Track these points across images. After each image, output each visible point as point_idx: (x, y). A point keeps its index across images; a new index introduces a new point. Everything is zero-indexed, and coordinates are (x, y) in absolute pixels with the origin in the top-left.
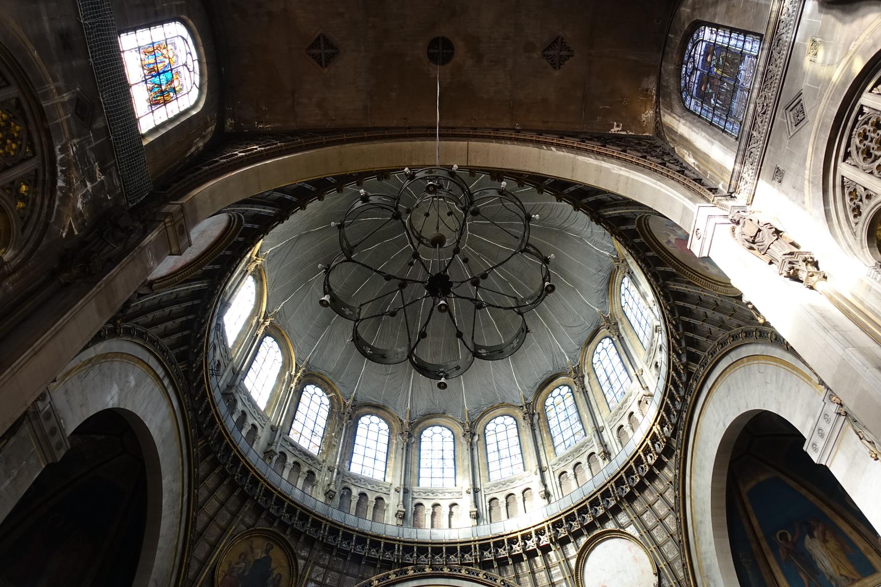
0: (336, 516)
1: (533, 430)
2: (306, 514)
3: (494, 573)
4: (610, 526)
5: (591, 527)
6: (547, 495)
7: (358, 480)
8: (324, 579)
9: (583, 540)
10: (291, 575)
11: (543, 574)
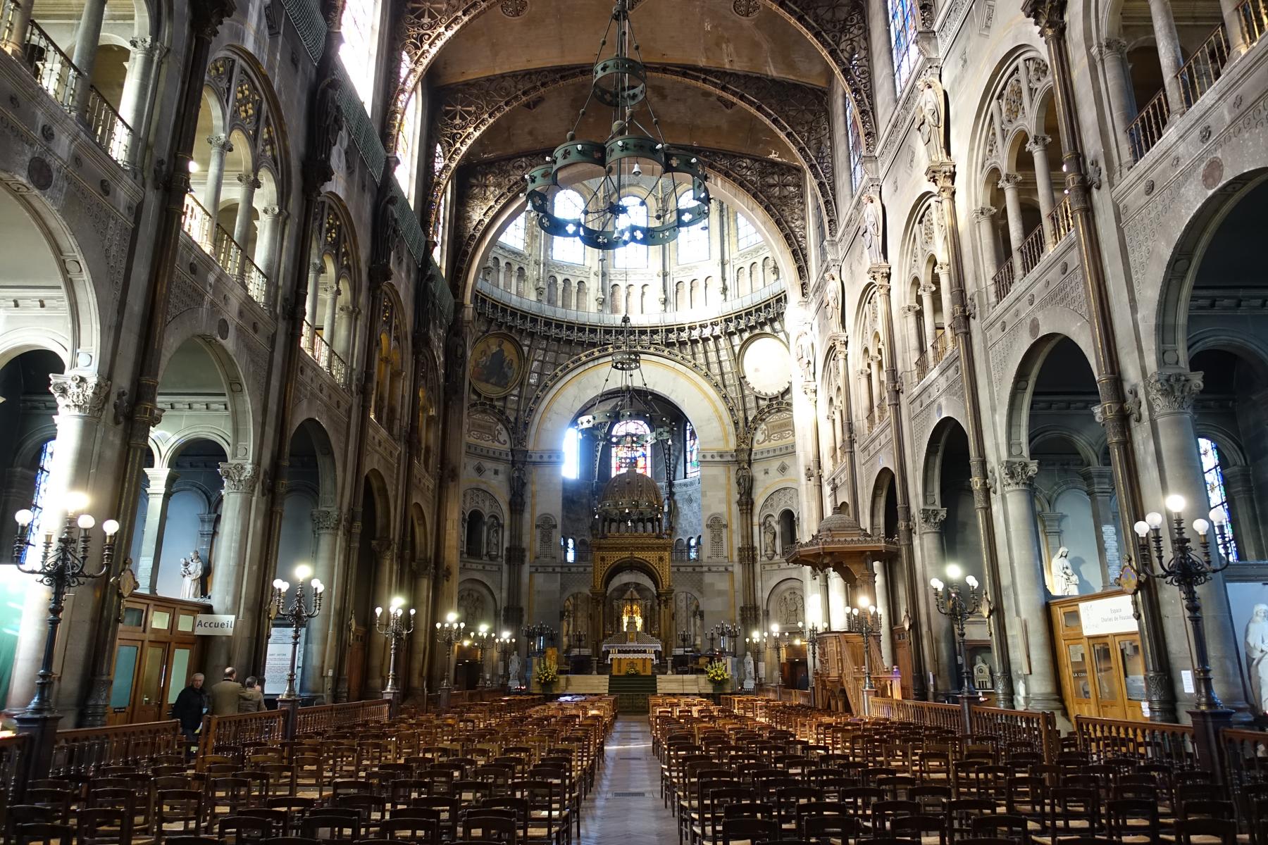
0: (548, 311)
1: (721, 217)
2: (524, 316)
3: (676, 351)
4: (767, 329)
5: (752, 328)
6: (725, 289)
7: (560, 266)
8: (545, 356)
9: (746, 335)
10: (519, 359)
11: (714, 354)
